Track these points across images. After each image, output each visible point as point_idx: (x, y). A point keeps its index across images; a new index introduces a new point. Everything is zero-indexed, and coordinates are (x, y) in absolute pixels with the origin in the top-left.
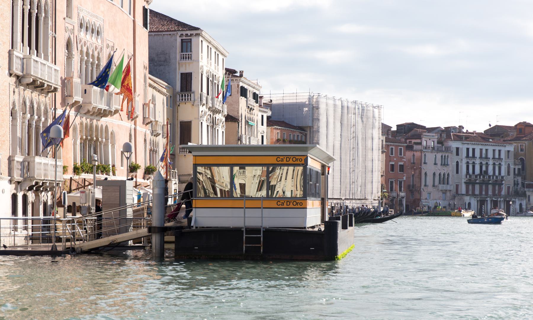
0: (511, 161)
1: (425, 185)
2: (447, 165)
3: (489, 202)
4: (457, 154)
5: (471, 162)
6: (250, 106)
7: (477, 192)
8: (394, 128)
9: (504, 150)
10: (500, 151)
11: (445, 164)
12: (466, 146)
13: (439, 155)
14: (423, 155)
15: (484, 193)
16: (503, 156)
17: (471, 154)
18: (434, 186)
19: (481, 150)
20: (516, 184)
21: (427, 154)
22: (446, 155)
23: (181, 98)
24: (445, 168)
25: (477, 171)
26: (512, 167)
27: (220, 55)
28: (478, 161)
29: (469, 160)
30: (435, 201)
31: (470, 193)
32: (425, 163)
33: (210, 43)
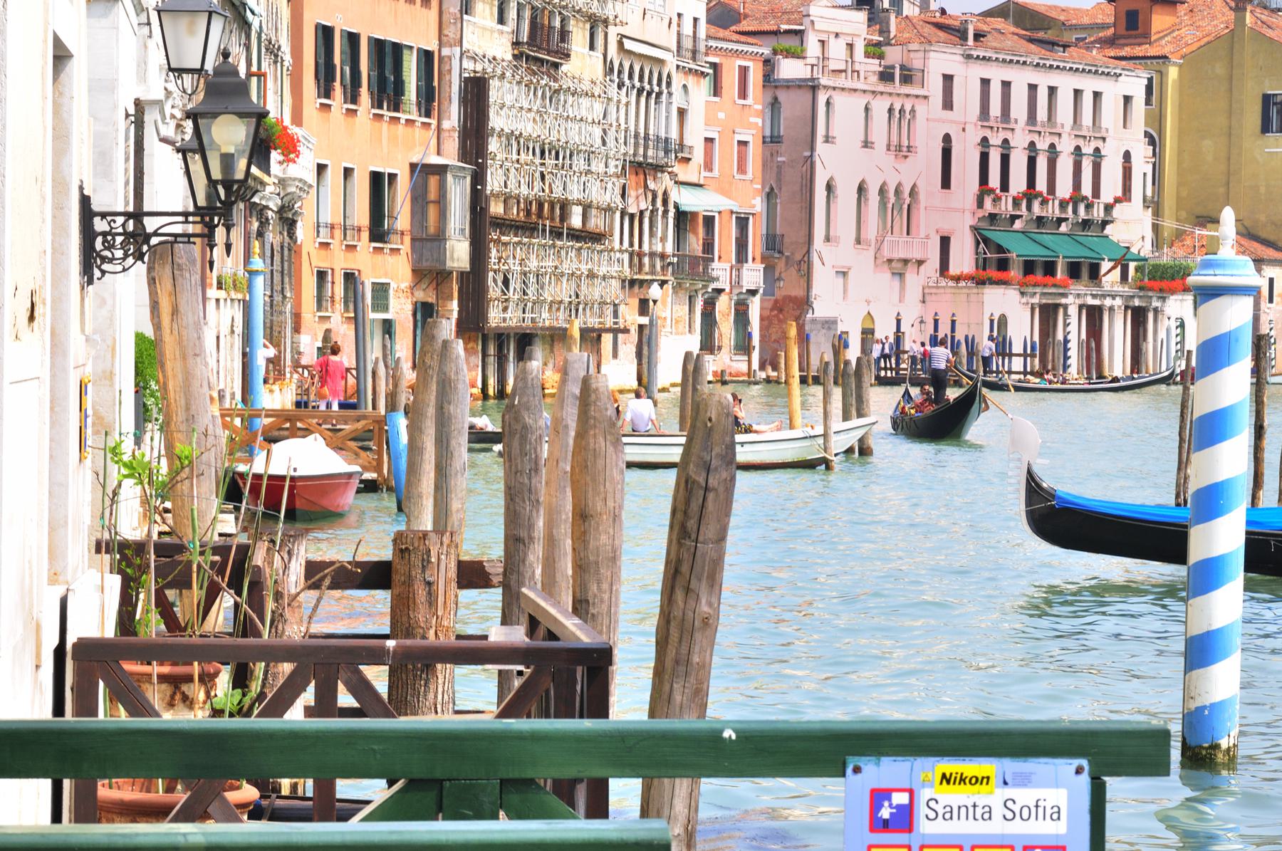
1: (828, 239)
3: (1073, 311)
4: (948, 104)
5: (996, 140)
9: (1112, 91)
17: (995, 109)
18: (858, 241)
21: (839, 100)
24: (904, 166)
25: (1018, 183)
28: (1020, 140)
29: (988, 133)
32: (828, 139)
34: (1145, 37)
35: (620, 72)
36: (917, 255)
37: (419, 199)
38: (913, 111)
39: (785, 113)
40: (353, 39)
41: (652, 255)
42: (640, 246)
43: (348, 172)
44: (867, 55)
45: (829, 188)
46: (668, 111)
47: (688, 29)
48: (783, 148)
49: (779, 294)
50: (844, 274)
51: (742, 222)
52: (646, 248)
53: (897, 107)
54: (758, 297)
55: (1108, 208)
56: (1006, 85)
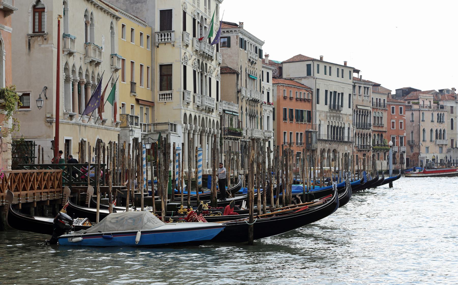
1: (424, 141)
2: (443, 122)
6: (252, 60)
14: (421, 113)
18: (431, 141)
21: (425, 112)
22: (442, 114)
23: (160, 38)
30: (433, 155)
32: (423, 121)
35: (357, 112)
36: (445, 143)
37: (307, 138)
38: (443, 114)
39: (414, 116)
40: (291, 110)
41: (367, 145)
42: (364, 143)
43: (291, 133)
44: (434, 103)
45: (424, 130)
46: (370, 118)
47: (382, 101)
48: (414, 123)
49: (414, 152)
50: (428, 148)
51: (401, 138)
52: (365, 144)
53: (439, 114)
54: (405, 154)
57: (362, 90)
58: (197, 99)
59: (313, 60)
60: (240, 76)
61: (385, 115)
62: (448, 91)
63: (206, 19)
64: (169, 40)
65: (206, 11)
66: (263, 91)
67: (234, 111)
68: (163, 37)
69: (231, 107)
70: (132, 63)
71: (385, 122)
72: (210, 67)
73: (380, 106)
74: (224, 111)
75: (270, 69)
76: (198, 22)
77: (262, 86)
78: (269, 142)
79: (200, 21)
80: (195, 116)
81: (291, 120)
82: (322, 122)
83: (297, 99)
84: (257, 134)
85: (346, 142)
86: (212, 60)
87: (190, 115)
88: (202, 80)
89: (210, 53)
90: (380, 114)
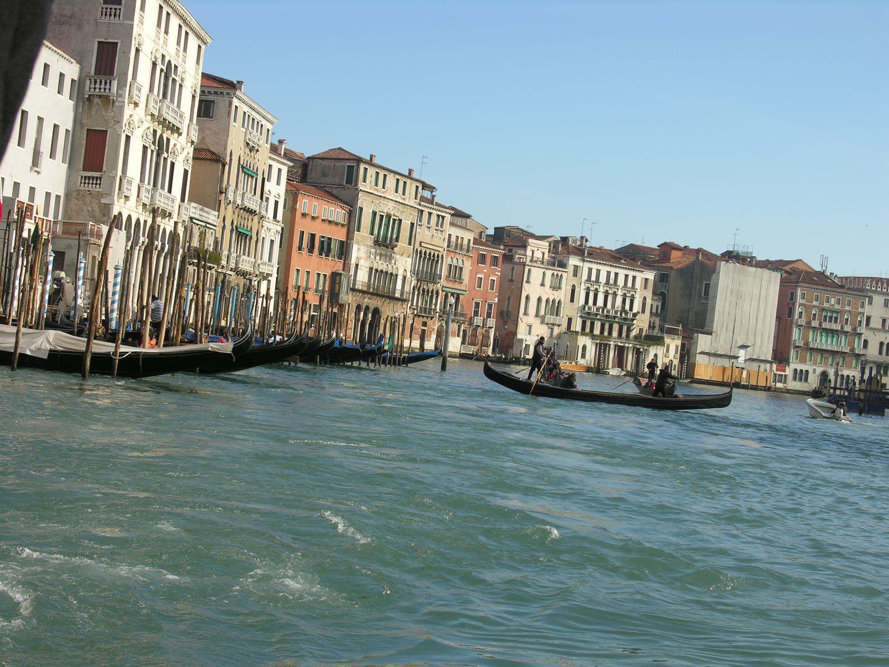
0: (649, 295)
1: (525, 314)
3: (612, 347)
4: (575, 275)
6: (251, 144)
7: (597, 331)
8: (491, 232)
9: (640, 277)
10: (634, 278)
11: (556, 287)
12: (587, 265)
13: (549, 273)
15: (606, 334)
16: (639, 284)
17: (593, 278)
18: (537, 315)
19: (609, 273)
20: (651, 327)
23: (93, 86)
25: (600, 302)
26: (649, 301)
27: (191, 37)
28: (601, 289)
31: (588, 330)
32: (528, 282)
33: (185, 21)
34: (669, 260)
45: (527, 298)
47: (465, 242)
50: (530, 326)
51: (490, 306)
55: (635, 315)
56: (598, 271)
57: (434, 219)
58: (143, 193)
59: (359, 160)
60: (227, 167)
61: (468, 266)
62: (574, 241)
63: (176, 67)
64: (107, 91)
65: (177, 55)
66: (267, 199)
67: (209, 221)
68: (98, 86)
69: (205, 215)
70: (40, 119)
71: (466, 275)
72: (175, 145)
73: (461, 249)
74: (191, 218)
75: (284, 164)
76: (162, 70)
77: (266, 189)
78: (269, 281)
79: (164, 68)
80: (138, 221)
81: (311, 250)
82: (362, 262)
83: (323, 220)
84: (246, 265)
85: (397, 299)
86: (180, 134)
87: (129, 217)
88: (157, 164)
89: (177, 124)
90: (460, 262)
